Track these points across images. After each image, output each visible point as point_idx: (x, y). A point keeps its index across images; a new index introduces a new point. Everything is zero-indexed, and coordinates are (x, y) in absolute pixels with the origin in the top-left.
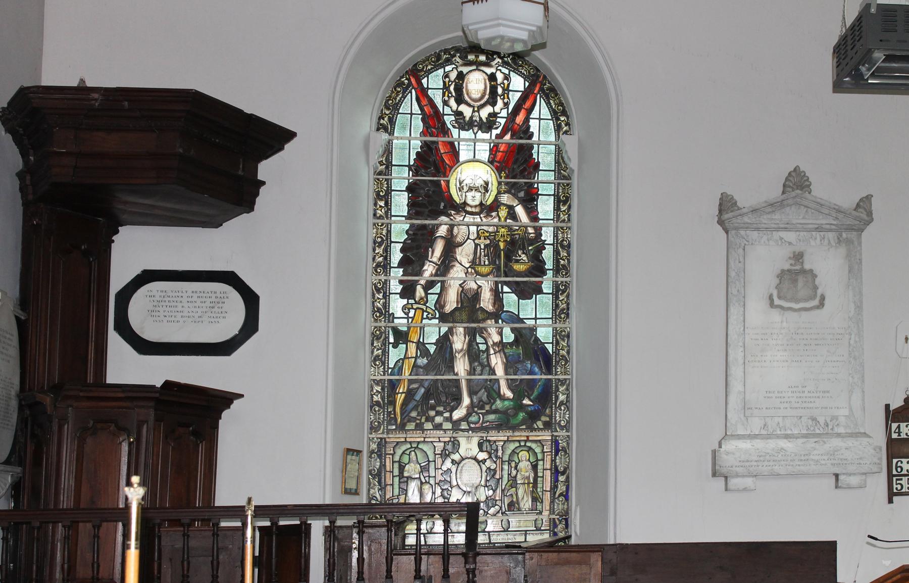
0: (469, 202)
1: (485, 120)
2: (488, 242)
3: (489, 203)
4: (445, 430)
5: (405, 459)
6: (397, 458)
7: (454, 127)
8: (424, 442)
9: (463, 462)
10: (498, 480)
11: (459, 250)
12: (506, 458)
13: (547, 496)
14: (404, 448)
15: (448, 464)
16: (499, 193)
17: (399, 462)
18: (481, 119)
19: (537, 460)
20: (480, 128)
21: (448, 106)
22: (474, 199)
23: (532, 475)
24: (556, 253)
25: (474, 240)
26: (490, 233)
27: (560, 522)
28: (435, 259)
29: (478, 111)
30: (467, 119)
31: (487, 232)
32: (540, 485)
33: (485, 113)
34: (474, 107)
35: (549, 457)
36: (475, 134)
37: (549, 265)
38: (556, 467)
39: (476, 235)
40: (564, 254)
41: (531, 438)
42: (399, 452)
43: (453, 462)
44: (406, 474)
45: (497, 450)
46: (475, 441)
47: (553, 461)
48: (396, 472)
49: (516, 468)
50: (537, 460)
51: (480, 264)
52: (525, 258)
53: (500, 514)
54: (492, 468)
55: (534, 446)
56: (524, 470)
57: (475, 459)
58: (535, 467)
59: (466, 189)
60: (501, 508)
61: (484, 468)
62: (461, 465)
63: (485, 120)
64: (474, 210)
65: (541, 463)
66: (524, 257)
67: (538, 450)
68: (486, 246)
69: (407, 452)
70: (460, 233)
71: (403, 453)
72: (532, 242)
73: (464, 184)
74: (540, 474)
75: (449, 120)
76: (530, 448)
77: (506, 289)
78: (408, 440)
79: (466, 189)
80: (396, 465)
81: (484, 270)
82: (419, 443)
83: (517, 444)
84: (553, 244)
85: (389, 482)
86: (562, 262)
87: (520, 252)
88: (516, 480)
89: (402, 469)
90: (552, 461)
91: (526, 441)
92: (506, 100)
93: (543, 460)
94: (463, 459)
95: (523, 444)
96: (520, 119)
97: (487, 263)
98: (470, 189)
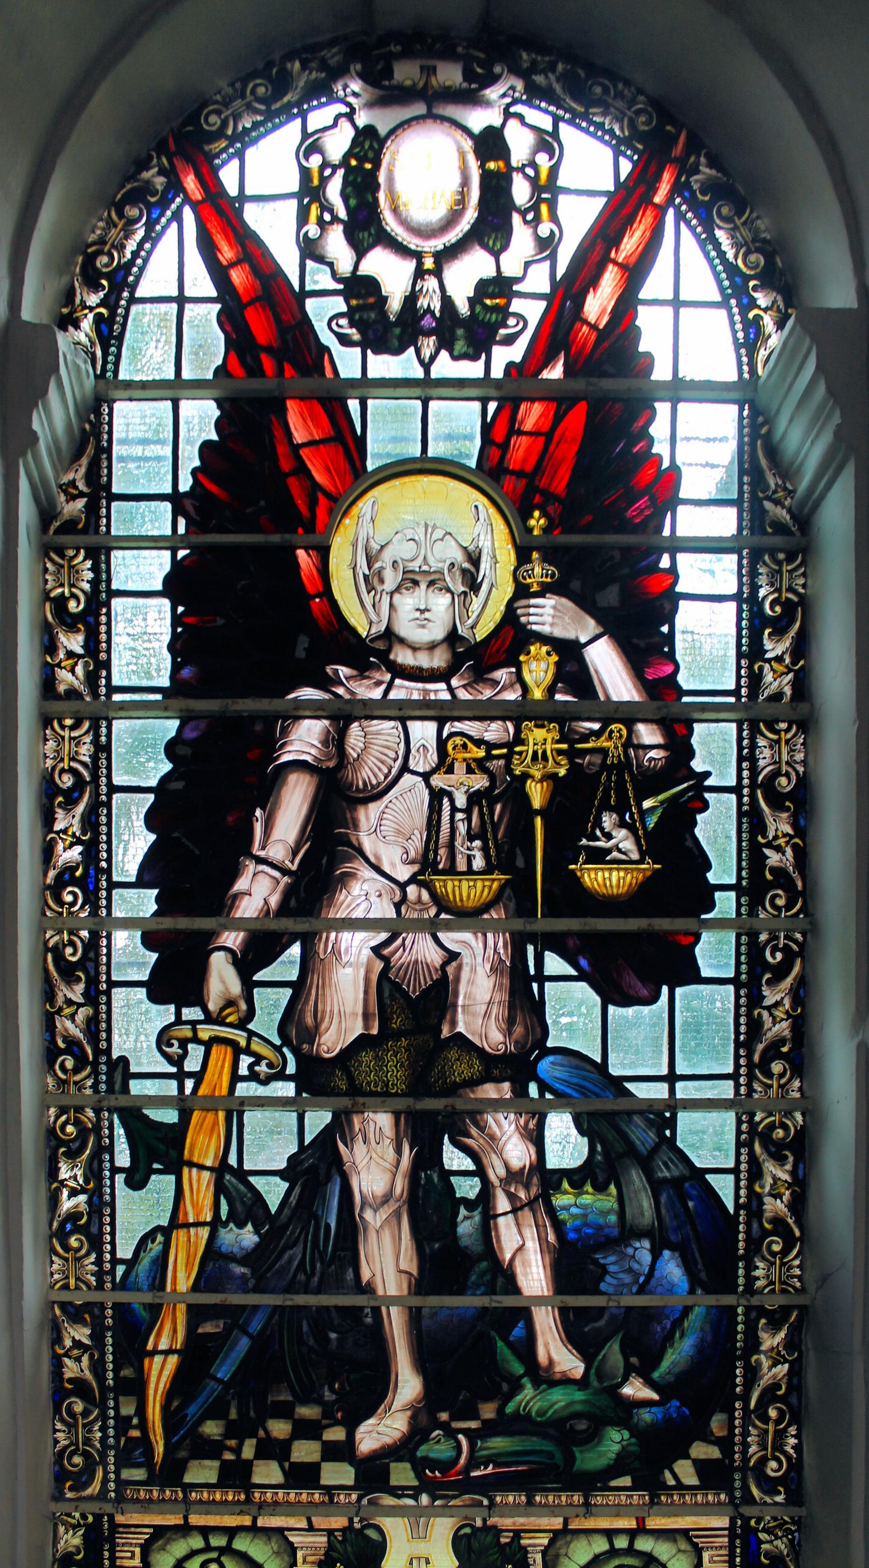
0: (405, 628)
1: (463, 308)
2: (480, 782)
3: (481, 633)
7: (345, 341)
11: (368, 815)
16: (522, 591)
18: (447, 302)
20: (445, 343)
21: (320, 259)
22: (423, 619)
24: (751, 821)
25: (426, 777)
26: (490, 746)
28: (277, 852)
29: (438, 272)
30: (395, 305)
31: (479, 743)
33: (464, 277)
34: (418, 256)
36: (427, 366)
37: (723, 870)
39: (433, 757)
40: (779, 825)
51: (451, 870)
52: (628, 845)
59: (391, 579)
63: (463, 308)
64: (424, 661)
66: (624, 841)
68: (474, 798)
70: (374, 745)
72: (652, 781)
73: (387, 557)
75: (324, 312)
77: (554, 964)
79: (391, 579)
81: (470, 891)
84: (737, 790)
86: (773, 858)
87: (608, 820)
92: (544, 229)
96: (597, 305)
97: (479, 863)
98: (410, 581)
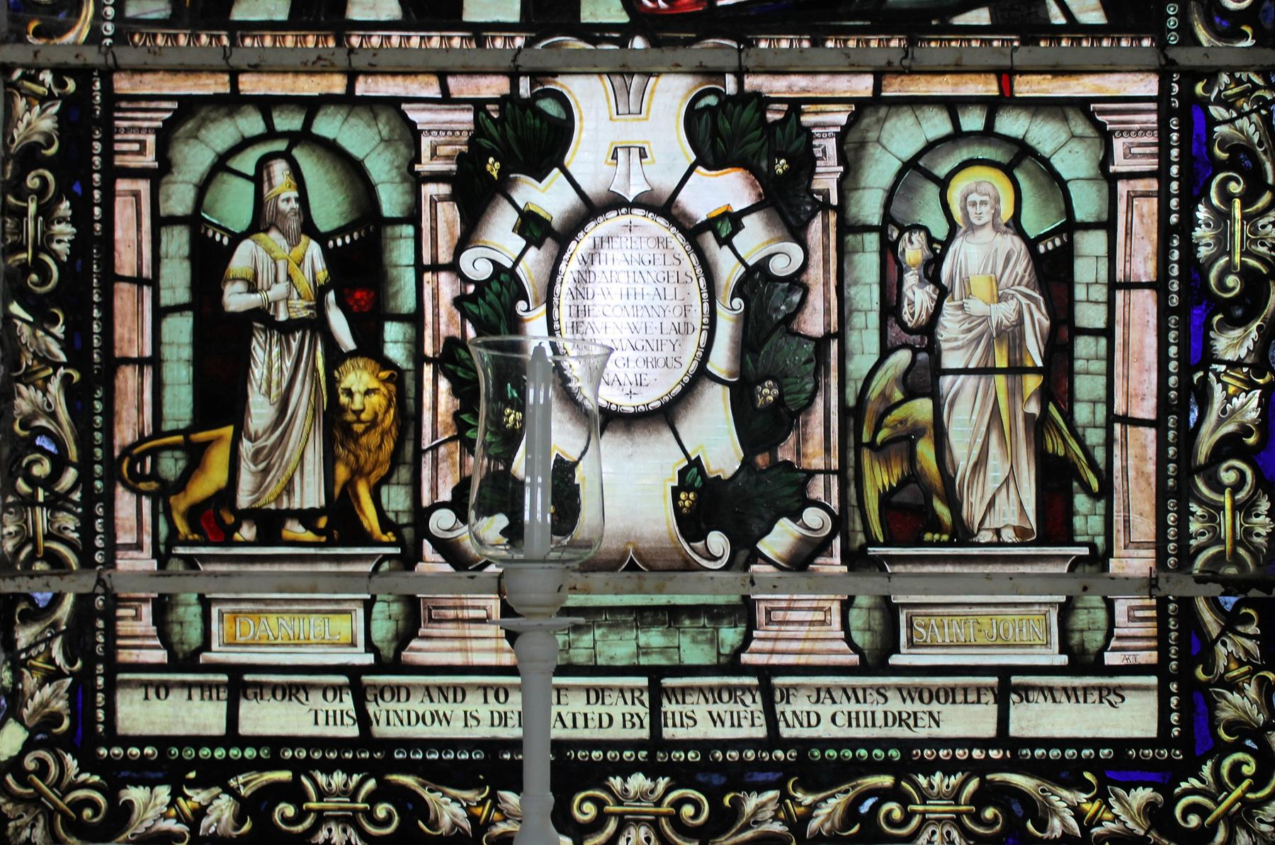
4: (479, 32)
5: (234, 204)
6: (179, 200)
8: (349, 102)
9: (595, 230)
10: (821, 344)
12: (869, 207)
13: (1138, 456)
14: (222, 134)
15: (502, 236)
17: (195, 221)
19: (1070, 226)
23: (1038, 320)
27: (1231, 622)
32: (1088, 386)
35: (1150, 207)
38: (1194, 269)
41: (1026, 87)
42: (195, 158)
43: (533, 227)
44: (236, 299)
45: (805, 163)
46: (671, 94)
47: (1174, 232)
48: (177, 282)
49: (931, 270)
50: (1070, 226)
53: (832, 564)
54: (780, 267)
55: (1044, 135)
56: (981, 286)
57: (663, 207)
58: (1052, 271)
60: (840, 523)
61: (729, 270)
62: (580, 247)
65: (1091, 244)
67: (1074, 162)
69: (247, 162)
71: (221, 165)
74: (1090, 315)
76: (1022, 151)
78: (250, 85)
80: (177, 242)
82: (311, 106)
83: (938, 124)
85: (132, 336)
88: (933, 350)
89: (210, 261)
90: (1165, 231)
91: (992, 106)
93: (1108, 225)
94: (592, 208)
95: (973, 121)
